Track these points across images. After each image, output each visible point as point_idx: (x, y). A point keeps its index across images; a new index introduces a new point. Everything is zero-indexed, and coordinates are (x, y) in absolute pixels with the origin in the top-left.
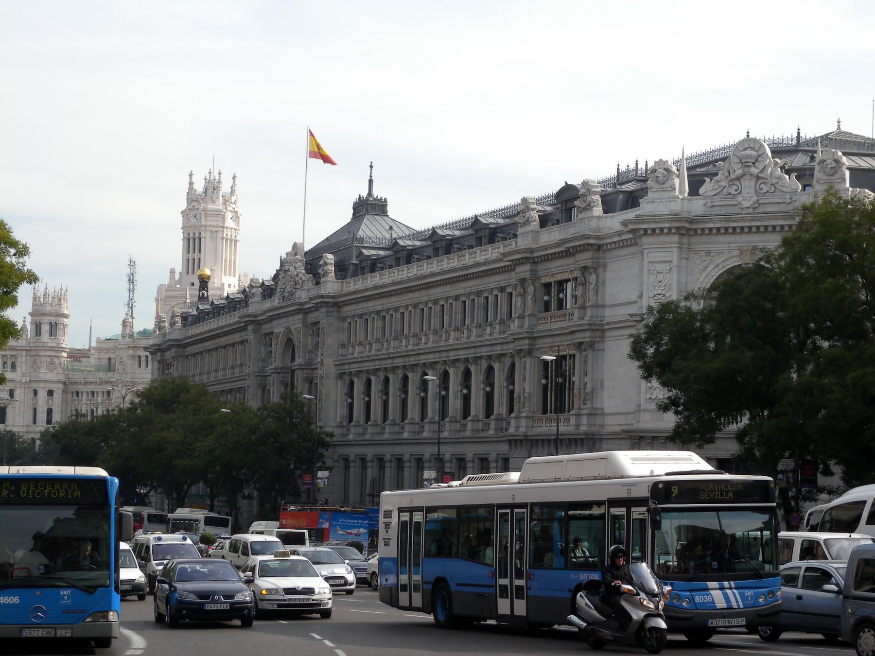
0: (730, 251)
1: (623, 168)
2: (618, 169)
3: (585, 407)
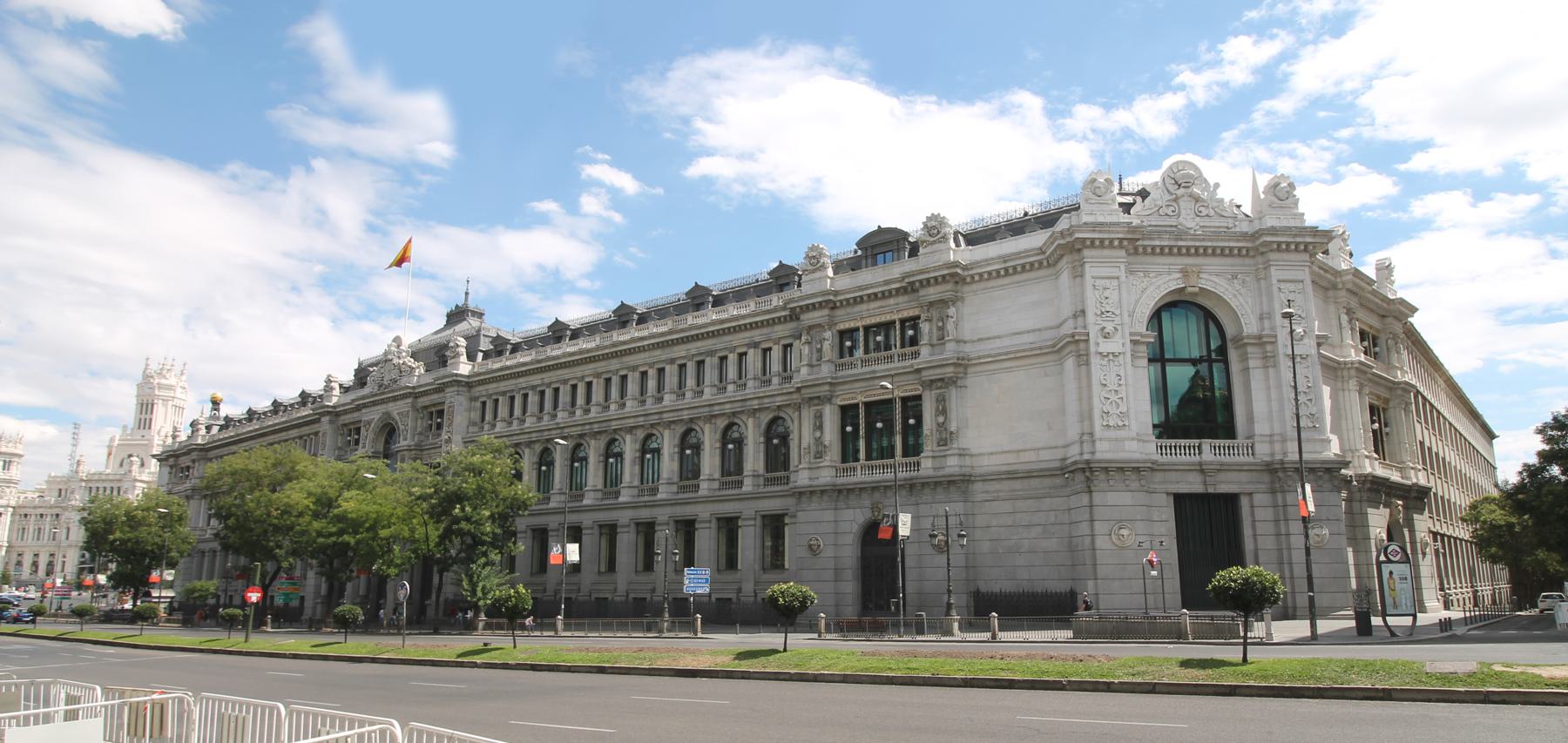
0: (1169, 273)
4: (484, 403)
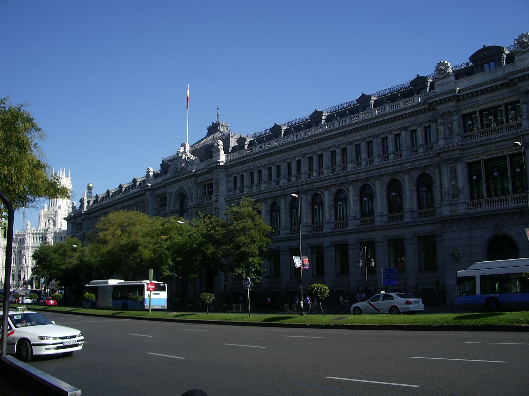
4: (235, 178)
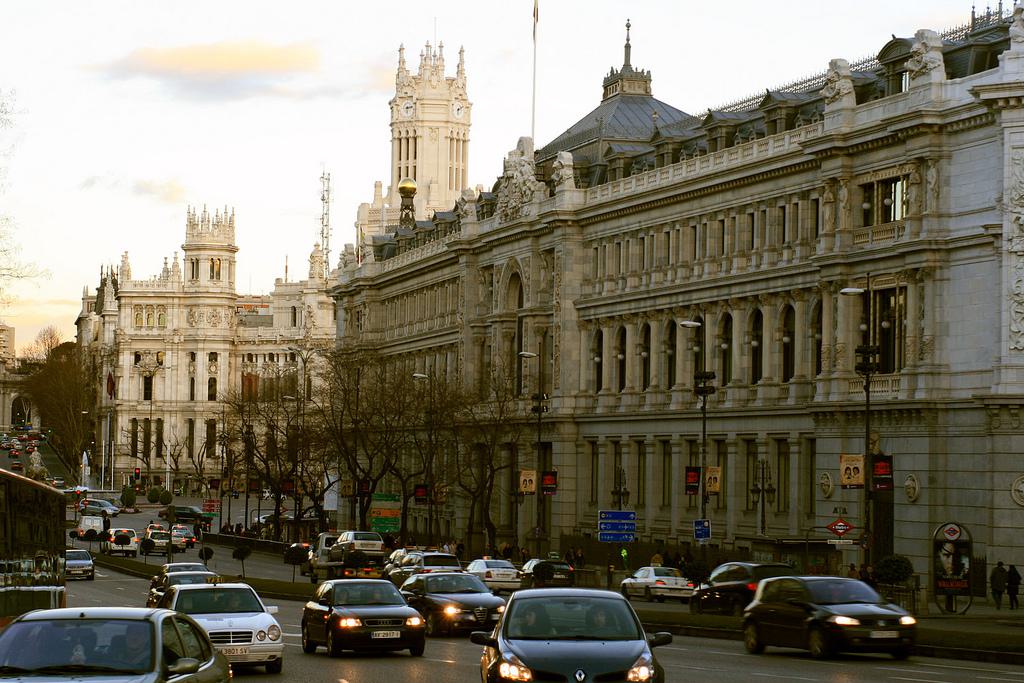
1: (980, 12)
2: (973, 13)
3: (921, 363)
